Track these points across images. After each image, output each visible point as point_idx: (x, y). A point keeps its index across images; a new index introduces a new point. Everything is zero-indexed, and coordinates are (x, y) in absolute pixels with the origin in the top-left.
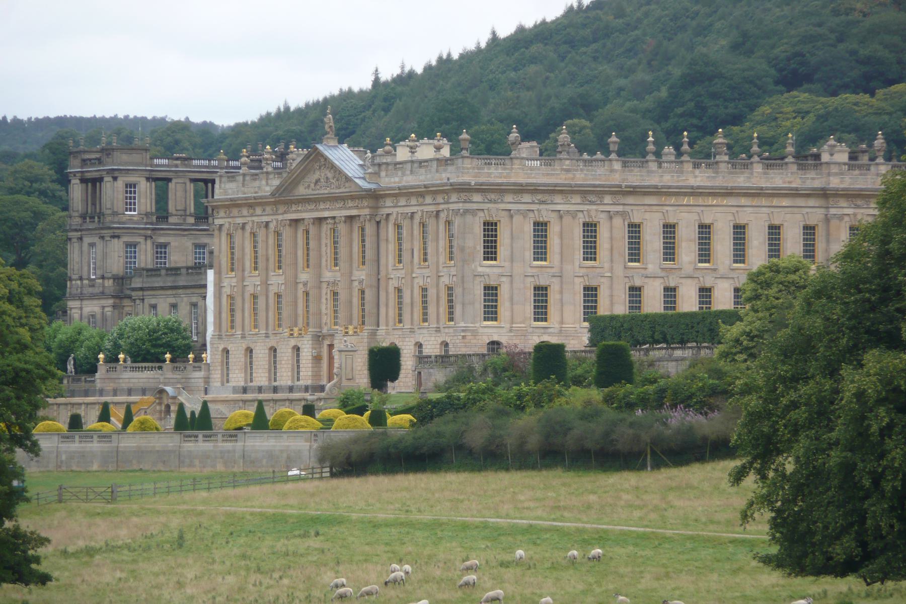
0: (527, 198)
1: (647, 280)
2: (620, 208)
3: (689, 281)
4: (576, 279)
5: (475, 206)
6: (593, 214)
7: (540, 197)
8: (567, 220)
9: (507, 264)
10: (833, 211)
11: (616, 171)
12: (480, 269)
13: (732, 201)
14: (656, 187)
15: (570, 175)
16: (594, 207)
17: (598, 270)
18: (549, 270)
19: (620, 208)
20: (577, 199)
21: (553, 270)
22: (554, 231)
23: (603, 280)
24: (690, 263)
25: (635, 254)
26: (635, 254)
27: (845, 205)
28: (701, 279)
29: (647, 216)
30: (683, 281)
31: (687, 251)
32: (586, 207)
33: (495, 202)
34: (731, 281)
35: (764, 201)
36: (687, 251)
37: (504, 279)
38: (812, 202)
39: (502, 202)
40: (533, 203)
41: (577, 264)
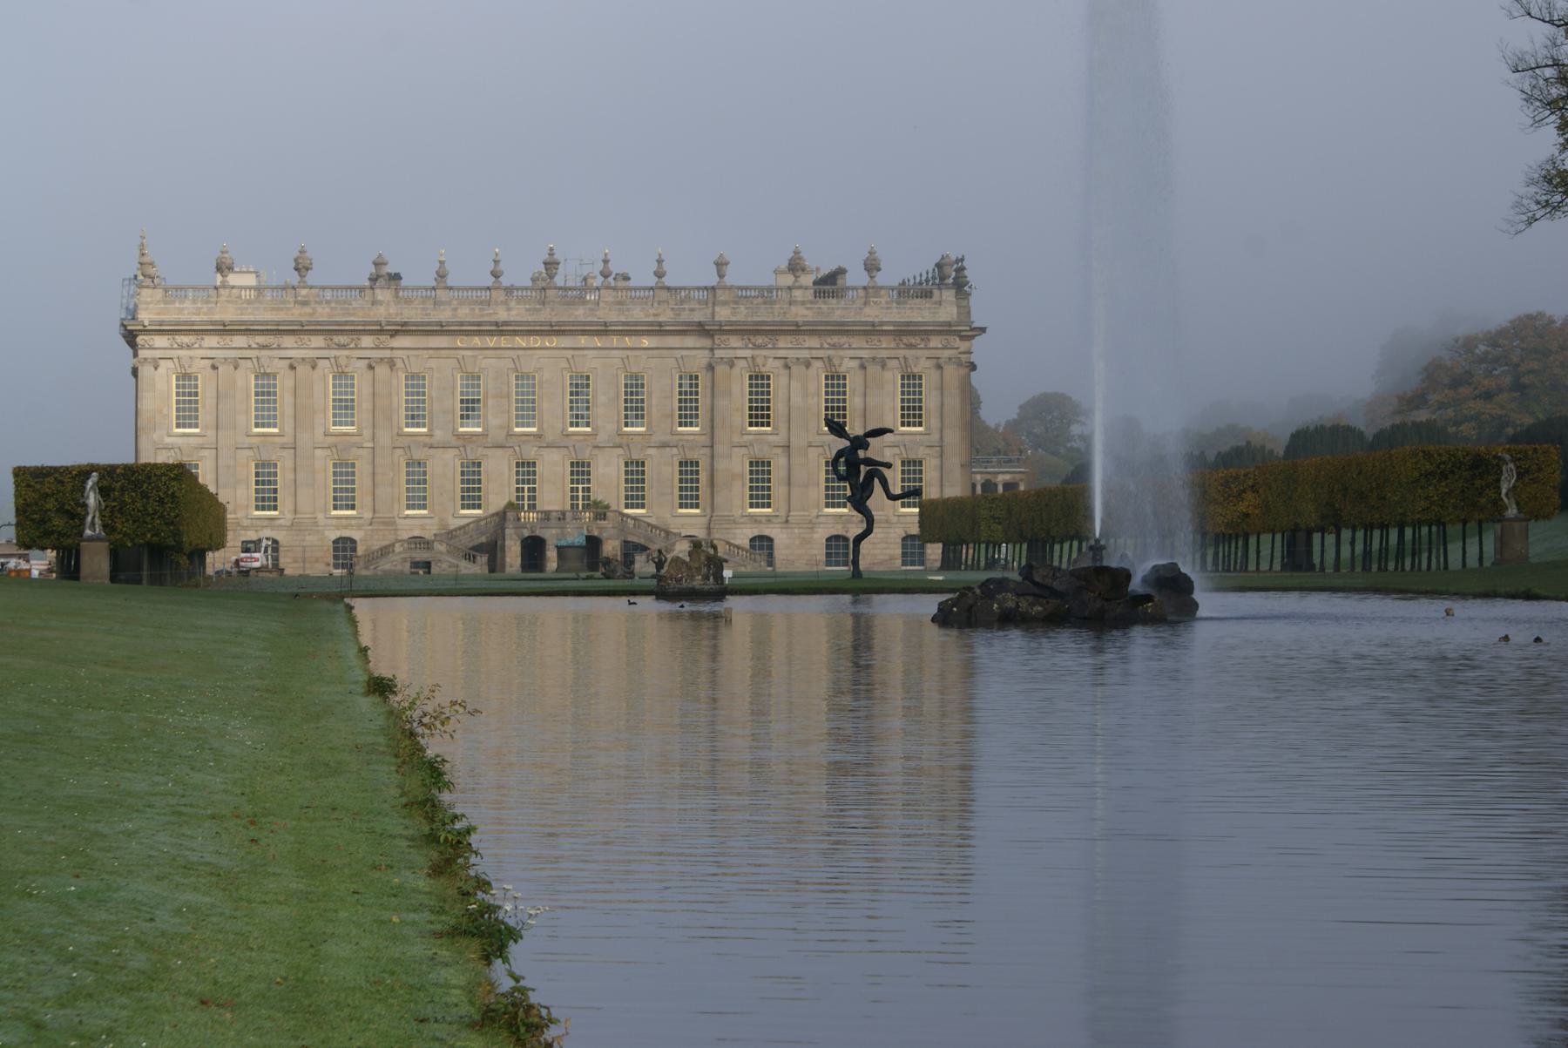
1: (432, 451)
2: (387, 354)
3: (499, 452)
4: (318, 452)
5: (158, 354)
6: (343, 362)
7: (261, 339)
9: (211, 433)
11: (381, 303)
12: (168, 440)
13: (566, 341)
15: (308, 310)
16: (346, 352)
18: (276, 439)
19: (387, 354)
20: (318, 341)
22: (284, 383)
23: (361, 452)
29: (433, 364)
30: (489, 452)
32: (333, 353)
33: (189, 347)
34: (565, 451)
35: (615, 341)
37: (206, 453)
38: (690, 341)
39: (201, 347)
40: (250, 348)
41: (319, 431)
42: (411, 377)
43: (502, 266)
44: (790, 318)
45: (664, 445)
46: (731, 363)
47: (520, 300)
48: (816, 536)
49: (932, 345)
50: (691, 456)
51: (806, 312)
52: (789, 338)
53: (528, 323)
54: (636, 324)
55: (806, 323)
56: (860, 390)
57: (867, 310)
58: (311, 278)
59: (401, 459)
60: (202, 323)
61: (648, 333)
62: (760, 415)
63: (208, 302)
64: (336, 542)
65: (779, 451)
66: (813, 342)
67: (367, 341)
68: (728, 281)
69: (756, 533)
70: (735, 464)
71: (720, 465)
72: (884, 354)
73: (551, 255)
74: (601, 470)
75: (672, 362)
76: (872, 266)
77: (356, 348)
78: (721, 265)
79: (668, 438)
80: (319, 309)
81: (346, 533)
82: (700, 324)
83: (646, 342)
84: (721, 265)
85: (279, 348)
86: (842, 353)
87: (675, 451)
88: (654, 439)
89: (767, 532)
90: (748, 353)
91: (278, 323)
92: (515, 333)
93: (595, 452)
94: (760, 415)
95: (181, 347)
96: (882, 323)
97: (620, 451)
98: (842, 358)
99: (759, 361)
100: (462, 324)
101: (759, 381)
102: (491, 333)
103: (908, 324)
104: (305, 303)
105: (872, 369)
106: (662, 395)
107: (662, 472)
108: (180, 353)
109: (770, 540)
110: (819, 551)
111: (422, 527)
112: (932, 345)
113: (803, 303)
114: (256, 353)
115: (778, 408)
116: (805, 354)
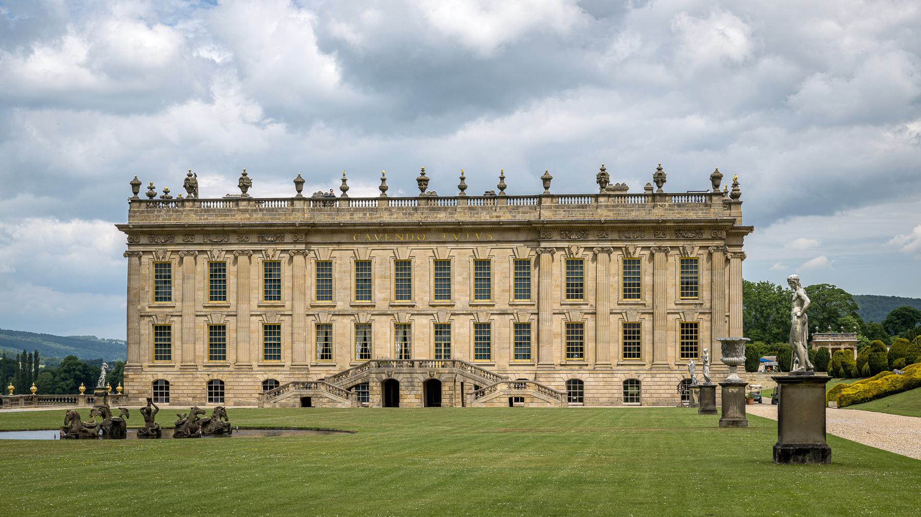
0: (198, 239)
4: (253, 318)
6: (270, 253)
8: (243, 259)
10: (543, 245)
14: (338, 225)
17: (279, 309)
19: (302, 247)
20: (254, 239)
21: (229, 310)
22: (231, 269)
24: (385, 300)
25: (325, 289)
26: (325, 289)
27: (558, 238)
28: (396, 316)
29: (335, 254)
31: (383, 289)
33: (163, 244)
36: (383, 289)
37: (175, 319)
42: (319, 264)
43: (387, 183)
44: (597, 218)
46: (551, 252)
48: (614, 379)
49: (704, 236)
50: (524, 319)
51: (611, 214)
52: (596, 233)
53: (402, 224)
54: (481, 223)
55: (606, 222)
56: (650, 270)
57: (655, 211)
59: (311, 322)
61: (491, 230)
65: (589, 316)
68: (551, 191)
69: (570, 377)
70: (553, 329)
71: (544, 327)
73: (423, 174)
74: (457, 331)
75: (430, 253)
78: (546, 180)
80: (255, 216)
81: (271, 376)
82: (529, 223)
83: (491, 237)
84: (546, 180)
87: (512, 317)
88: (496, 307)
89: (578, 377)
91: (223, 226)
92: (394, 231)
93: (452, 317)
94: (575, 289)
95: (157, 244)
96: (665, 221)
97: (471, 317)
98: (165, 252)
99: (574, 250)
100: (355, 225)
101: (575, 265)
102: (377, 232)
105: (659, 256)
107: (503, 334)
109: (581, 382)
110: (619, 392)
112: (704, 236)
113: (607, 206)
115: (589, 284)
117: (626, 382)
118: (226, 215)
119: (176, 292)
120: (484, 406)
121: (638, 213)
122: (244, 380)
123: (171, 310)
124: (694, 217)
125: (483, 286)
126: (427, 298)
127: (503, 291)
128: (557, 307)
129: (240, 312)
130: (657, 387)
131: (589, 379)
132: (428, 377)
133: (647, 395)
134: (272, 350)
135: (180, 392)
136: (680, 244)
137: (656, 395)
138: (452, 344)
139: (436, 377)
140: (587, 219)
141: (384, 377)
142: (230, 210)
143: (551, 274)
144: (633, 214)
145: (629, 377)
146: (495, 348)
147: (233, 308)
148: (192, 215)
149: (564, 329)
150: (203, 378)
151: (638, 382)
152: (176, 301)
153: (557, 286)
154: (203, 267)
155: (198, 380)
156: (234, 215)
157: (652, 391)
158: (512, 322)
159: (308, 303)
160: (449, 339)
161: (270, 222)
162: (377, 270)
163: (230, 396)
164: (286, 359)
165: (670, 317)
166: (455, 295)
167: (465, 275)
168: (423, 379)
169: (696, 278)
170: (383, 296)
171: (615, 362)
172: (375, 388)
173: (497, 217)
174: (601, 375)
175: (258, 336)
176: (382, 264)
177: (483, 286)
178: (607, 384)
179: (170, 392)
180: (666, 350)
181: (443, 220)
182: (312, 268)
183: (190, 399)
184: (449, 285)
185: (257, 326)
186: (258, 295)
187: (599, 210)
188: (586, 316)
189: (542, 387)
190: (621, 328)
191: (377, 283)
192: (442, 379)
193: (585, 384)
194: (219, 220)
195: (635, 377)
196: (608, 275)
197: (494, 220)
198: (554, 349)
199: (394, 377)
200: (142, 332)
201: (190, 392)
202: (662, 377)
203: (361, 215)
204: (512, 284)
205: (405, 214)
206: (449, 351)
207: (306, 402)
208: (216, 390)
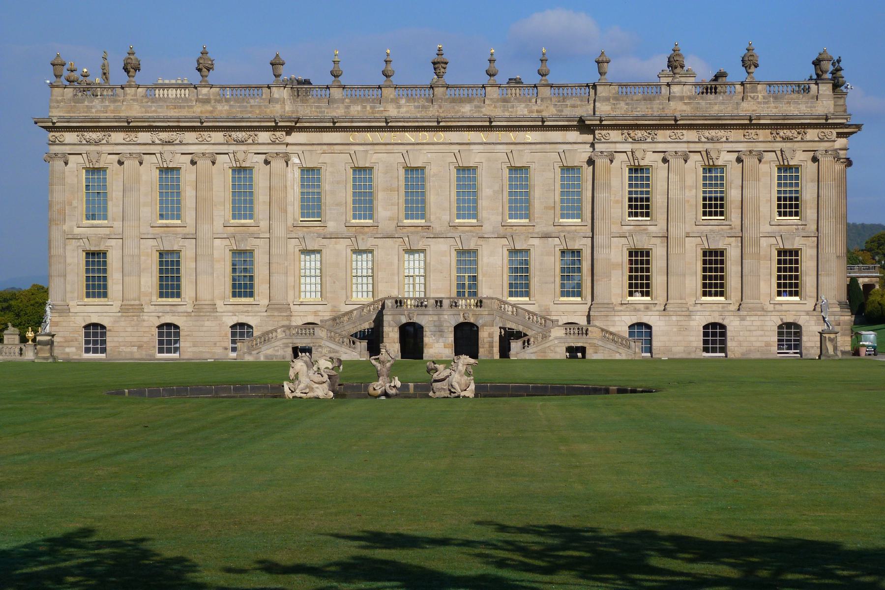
0: (144, 137)
2: (282, 149)
3: (389, 241)
5: (67, 149)
6: (240, 156)
7: (164, 136)
9: (118, 225)
11: (277, 101)
12: (77, 231)
15: (208, 108)
16: (244, 148)
19: (282, 149)
20: (218, 136)
24: (391, 219)
29: (327, 158)
30: (380, 242)
33: (97, 143)
37: (113, 242)
38: (573, 136)
39: (108, 143)
40: (153, 143)
42: (305, 170)
44: (669, 112)
45: (546, 236)
47: (410, 99)
48: (692, 323)
51: (685, 107)
52: (668, 132)
57: (744, 105)
58: (212, 77)
60: (107, 120)
62: (640, 206)
63: (115, 101)
64: (233, 327)
65: (658, 241)
66: (692, 135)
67: (264, 136)
70: (614, 257)
72: (761, 147)
76: (749, 63)
77: (253, 144)
79: (551, 229)
80: (219, 107)
82: (581, 120)
85: (181, 143)
86: (718, 146)
88: (537, 229)
89: (645, 320)
90: (628, 147)
93: (480, 242)
94: (640, 206)
95: (89, 143)
97: (504, 241)
98: (719, 152)
99: (638, 154)
103: (785, 117)
104: (207, 101)
106: (545, 187)
107: (545, 263)
108: (88, 148)
109: (649, 327)
110: (698, 340)
111: (316, 313)
113: (682, 98)
114: (160, 148)
115: (658, 201)
116: (683, 147)
117: (706, 327)
118: (180, 107)
119: (113, 208)
120: (533, 357)
121: (722, 107)
122: (207, 323)
123: (107, 231)
124: (796, 113)
125: (520, 202)
126: (446, 218)
127: (546, 208)
128: (615, 229)
129: (200, 234)
130: (747, 333)
131: (659, 323)
132: (461, 320)
133: (734, 344)
134: (243, 287)
135: (121, 339)
136: (778, 146)
137: (745, 344)
138: (480, 278)
139: (472, 320)
140: (656, 114)
141: (404, 320)
142: (185, 100)
143: (609, 186)
144: (716, 107)
145: (712, 320)
146: (535, 283)
147: (190, 229)
148: (136, 106)
149: (626, 258)
150: (152, 319)
151: (723, 327)
152: (114, 220)
153: (617, 202)
154: (149, 174)
155: (145, 324)
156: (191, 107)
157: (741, 339)
158: (557, 249)
159: (290, 222)
160: (476, 270)
161: (239, 115)
162: (379, 179)
163: (188, 344)
164: (261, 296)
165: (763, 240)
166: (483, 214)
167: (497, 187)
168: (454, 324)
169: (648, 193)
170: (388, 214)
171: (691, 301)
172: (391, 335)
173: (538, 111)
174: (674, 318)
175: (152, 265)
176: (386, 173)
177: (520, 202)
178: (683, 329)
179: (108, 339)
180: (758, 285)
181: (468, 114)
182: (294, 175)
183: (135, 349)
184: (475, 201)
185: (222, 251)
186: (222, 212)
187: (671, 103)
188: (654, 241)
189: (611, 333)
190: (700, 258)
191: (381, 197)
192: (480, 323)
193: (654, 329)
194: (173, 113)
195: (718, 320)
196: (683, 188)
197: (535, 115)
198: (615, 282)
199: (415, 320)
200: (69, 260)
201: (135, 339)
202: (752, 321)
203: (359, 108)
204: (558, 198)
205: (418, 107)
206: (476, 286)
207: (572, 351)
208: (169, 334)
